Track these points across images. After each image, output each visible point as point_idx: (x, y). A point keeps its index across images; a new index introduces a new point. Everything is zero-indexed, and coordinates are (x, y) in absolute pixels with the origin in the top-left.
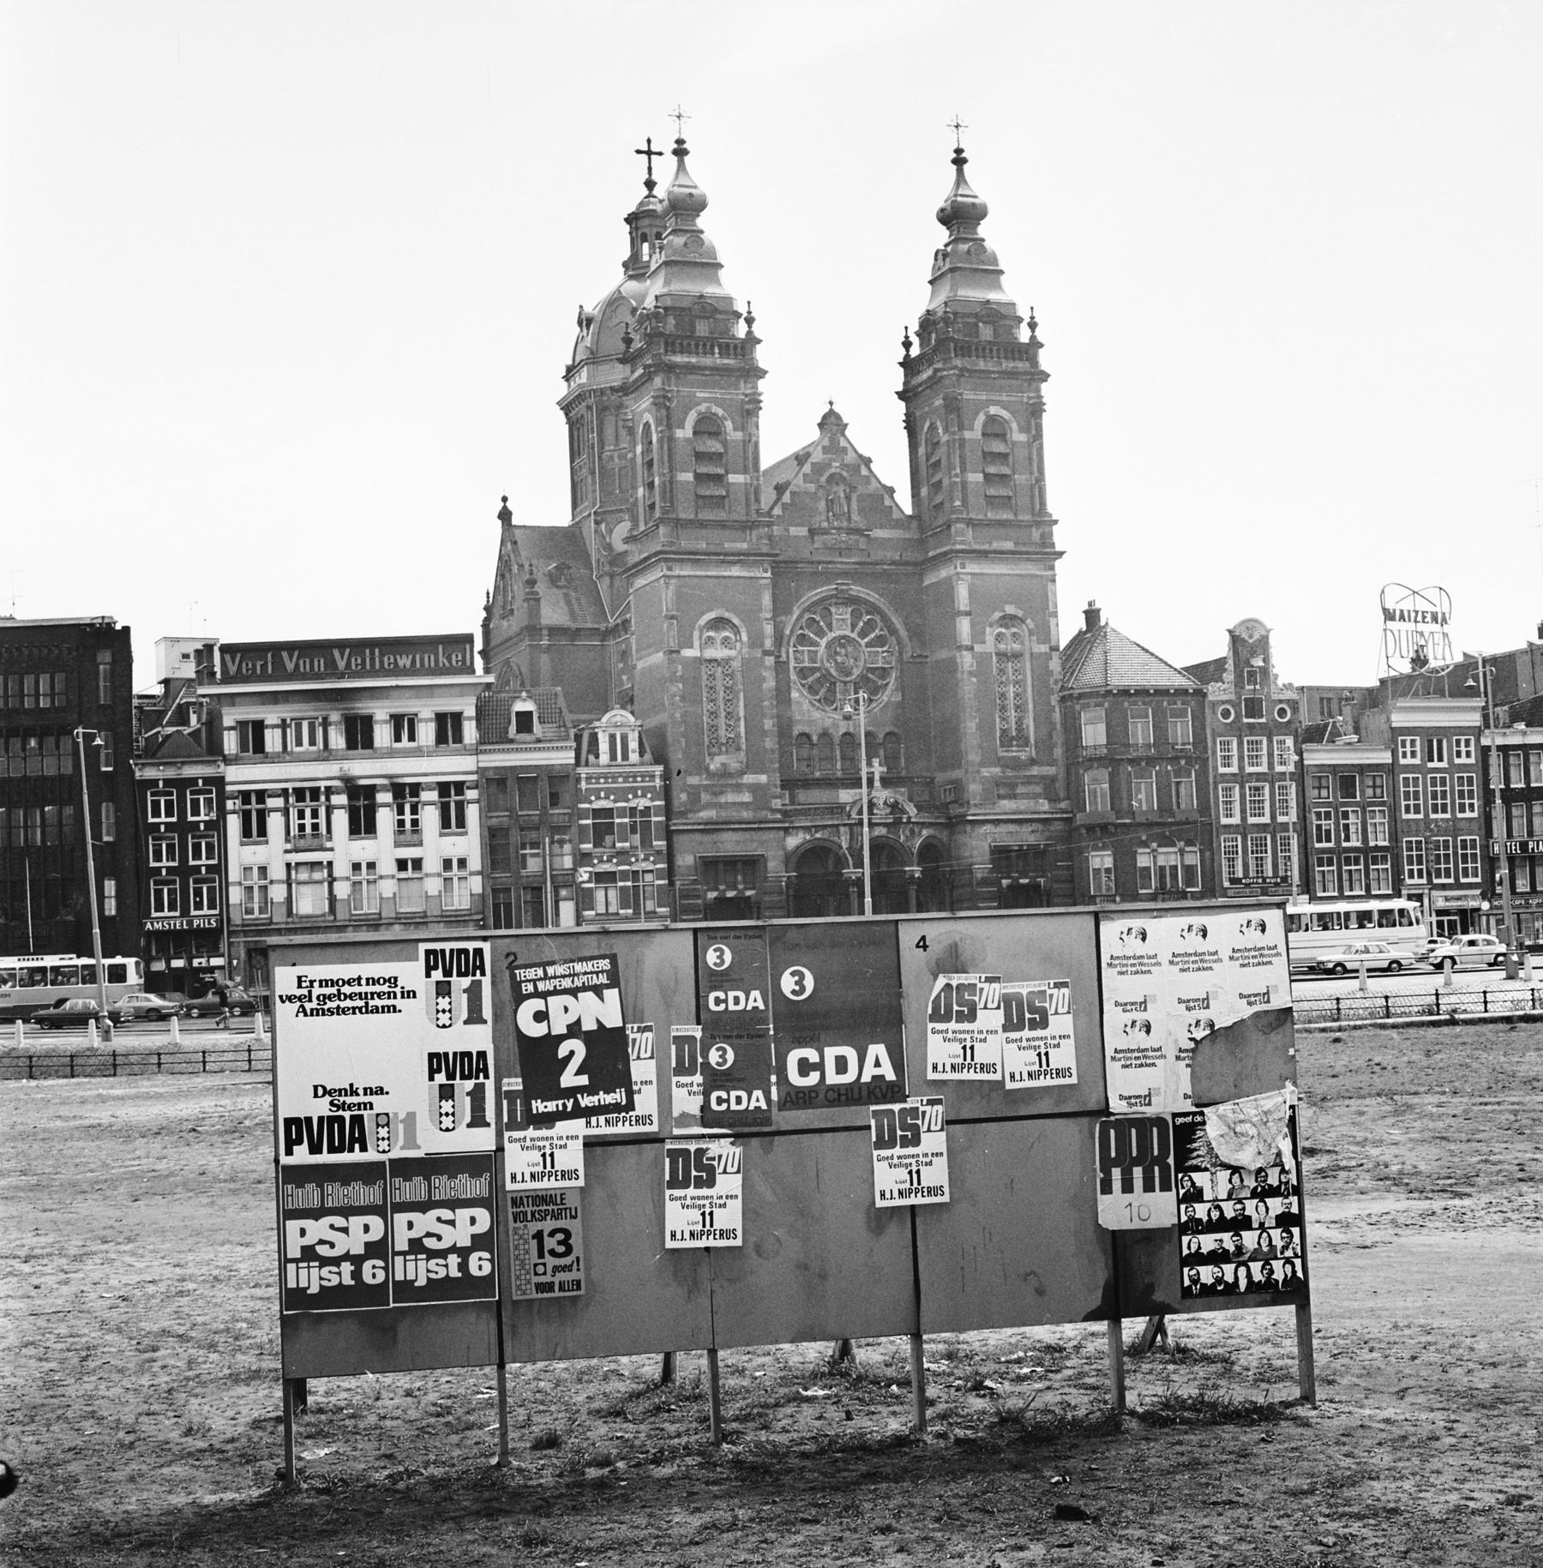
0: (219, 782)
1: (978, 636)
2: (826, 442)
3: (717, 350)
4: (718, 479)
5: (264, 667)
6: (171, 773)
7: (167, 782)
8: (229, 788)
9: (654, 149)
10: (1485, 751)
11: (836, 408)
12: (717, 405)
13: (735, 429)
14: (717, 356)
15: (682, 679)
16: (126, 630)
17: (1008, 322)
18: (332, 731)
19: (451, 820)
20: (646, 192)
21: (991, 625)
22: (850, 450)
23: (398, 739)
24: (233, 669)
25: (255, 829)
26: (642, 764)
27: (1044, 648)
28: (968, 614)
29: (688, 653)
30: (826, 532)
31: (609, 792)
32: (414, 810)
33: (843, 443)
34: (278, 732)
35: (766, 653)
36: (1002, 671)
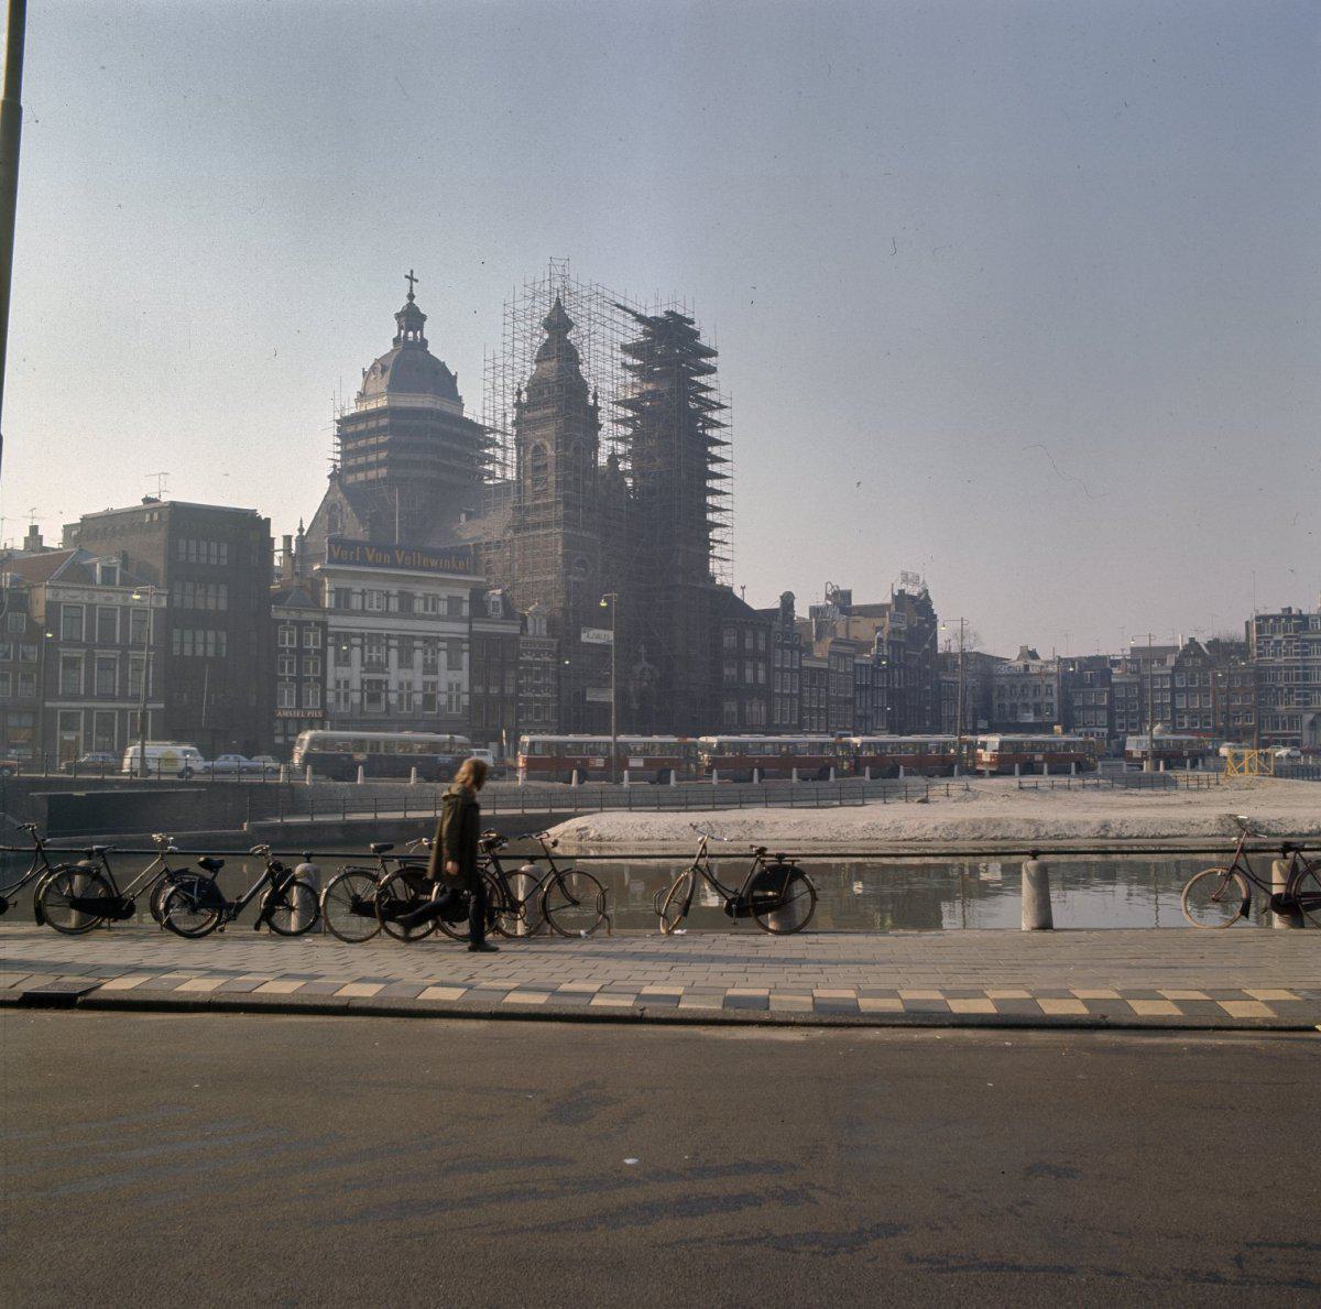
0: (324, 625)
5: (355, 556)
6: (294, 615)
7: (294, 622)
8: (330, 629)
9: (415, 276)
10: (856, 665)
16: (268, 520)
18: (391, 600)
19: (453, 665)
23: (426, 608)
24: (336, 555)
25: (344, 660)
26: (548, 637)
31: (532, 651)
32: (433, 654)
34: (360, 597)
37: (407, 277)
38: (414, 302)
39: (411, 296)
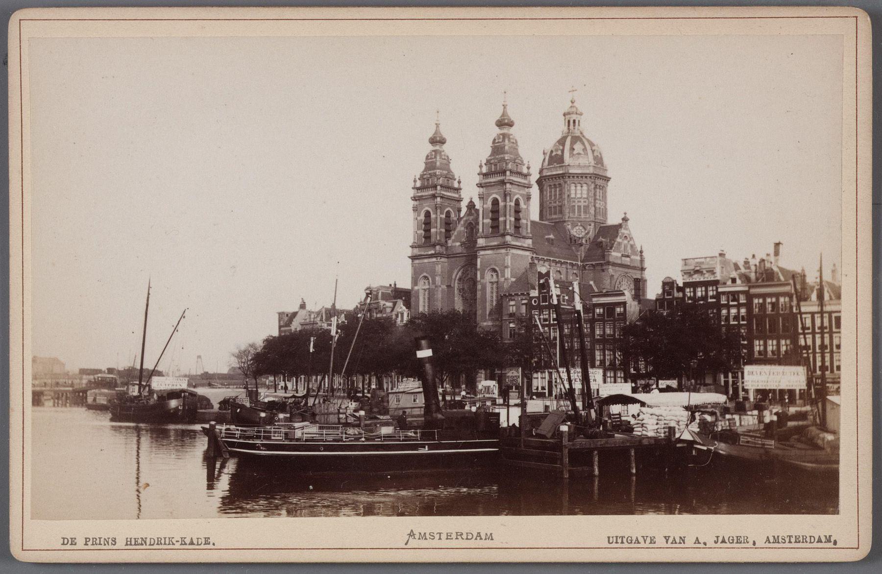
1: (483, 277)
9: (574, 89)
11: (473, 201)
20: (571, 104)
28: (479, 270)
38: (575, 104)
39: (572, 102)
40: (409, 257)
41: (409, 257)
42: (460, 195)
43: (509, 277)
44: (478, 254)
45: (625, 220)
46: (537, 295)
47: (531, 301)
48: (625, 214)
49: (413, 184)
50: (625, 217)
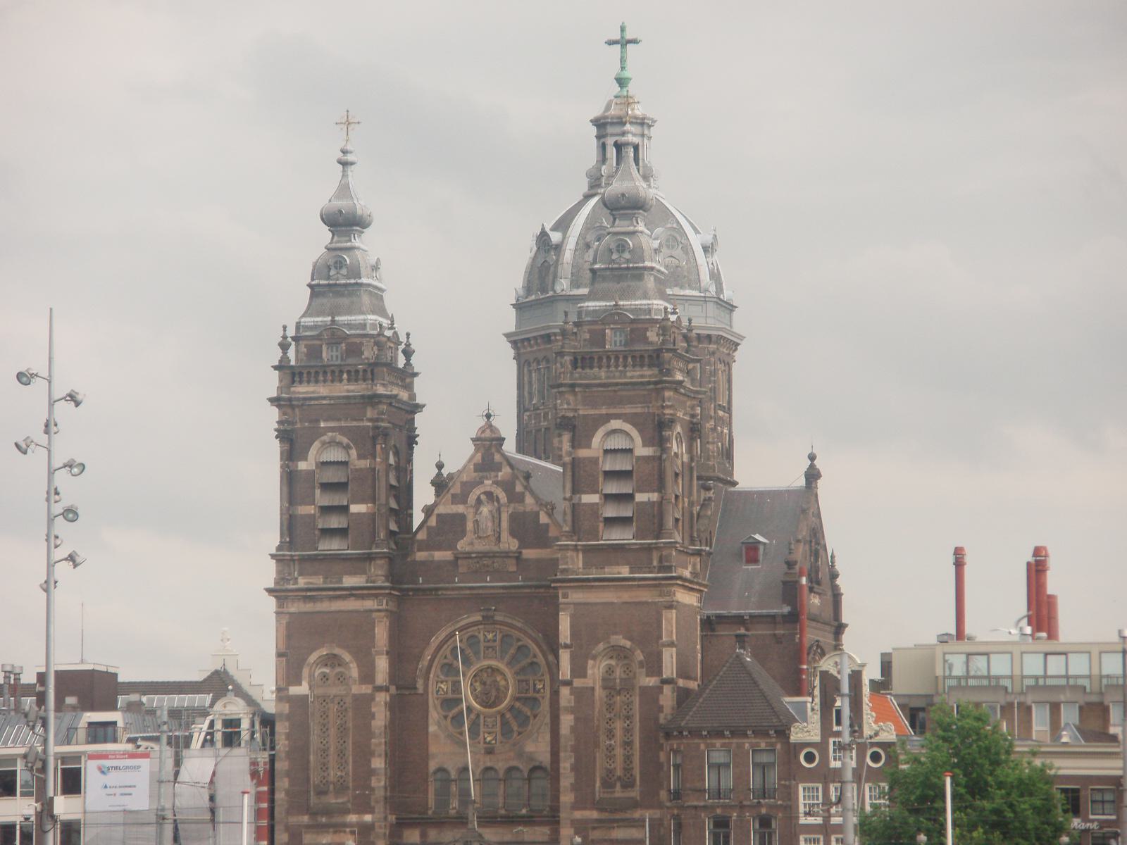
1: (578, 670)
2: (479, 455)
3: (345, 376)
4: (345, 509)
9: (629, 36)
11: (494, 422)
12: (344, 434)
13: (360, 457)
14: (345, 382)
15: (288, 718)
17: (640, 326)
20: (616, 89)
21: (594, 658)
22: (505, 463)
27: (651, 681)
28: (566, 646)
29: (294, 690)
30: (467, 556)
33: (497, 457)
35: (379, 689)
36: (610, 707)
37: (611, 43)
38: (632, 89)
40: (269, 591)
41: (269, 591)
42: (413, 397)
43: (675, 676)
44: (561, 600)
45: (812, 475)
46: (817, 739)
47: (797, 757)
48: (812, 458)
49: (279, 353)
50: (812, 467)
